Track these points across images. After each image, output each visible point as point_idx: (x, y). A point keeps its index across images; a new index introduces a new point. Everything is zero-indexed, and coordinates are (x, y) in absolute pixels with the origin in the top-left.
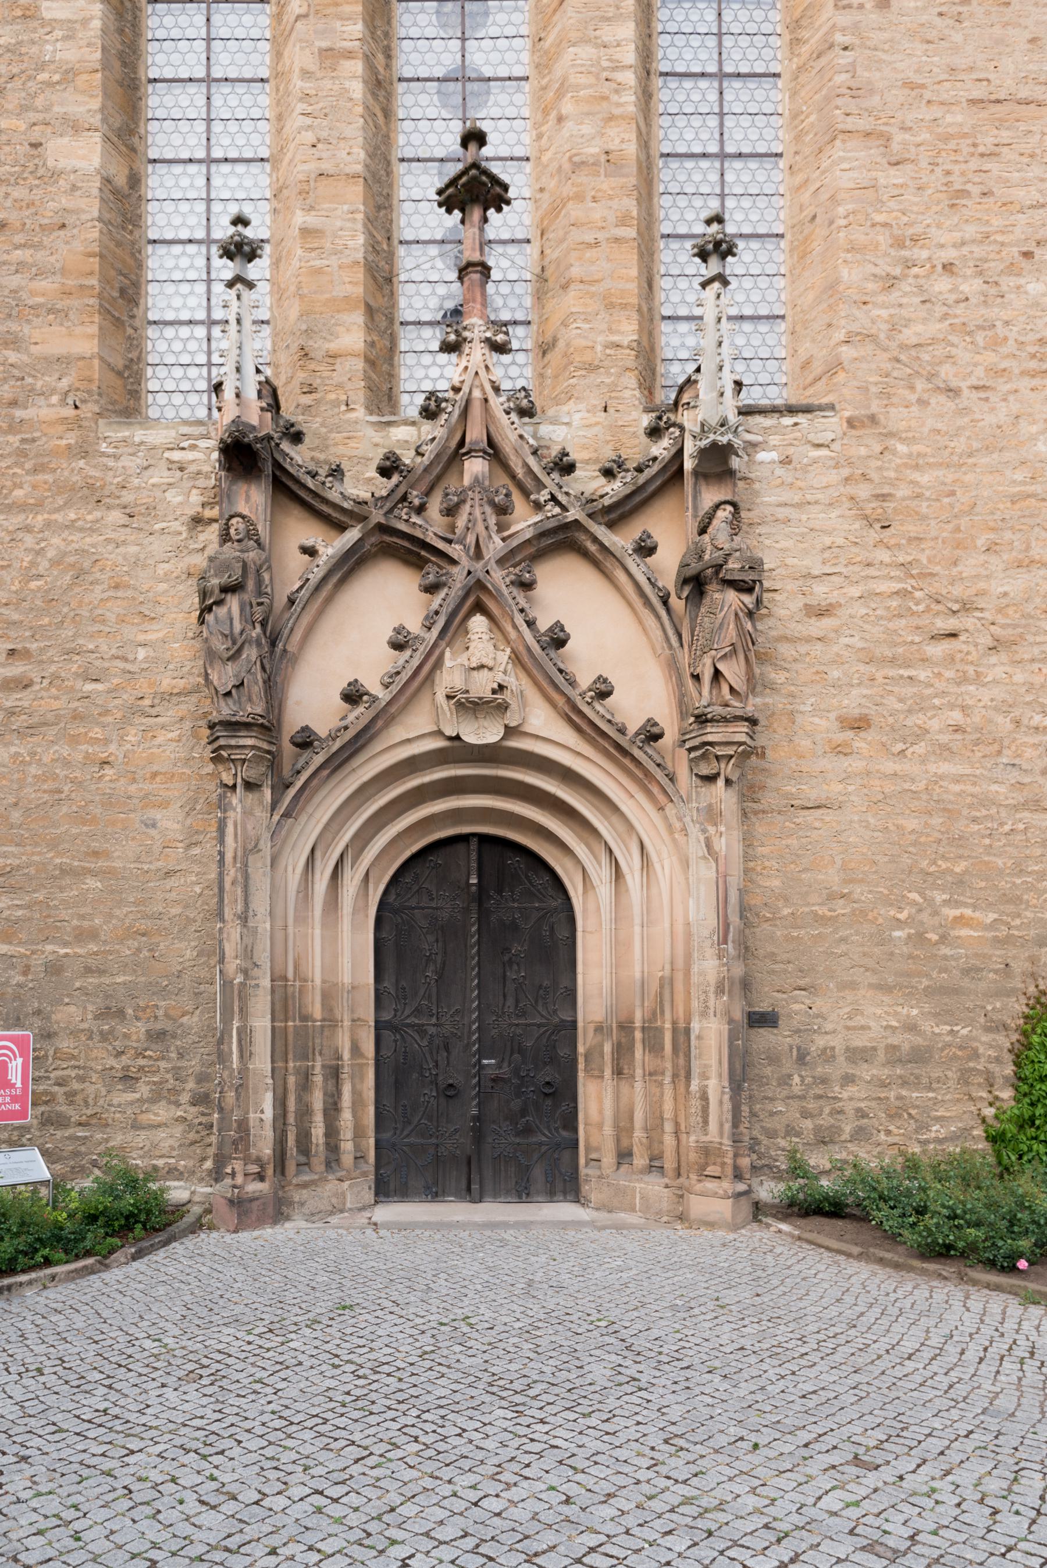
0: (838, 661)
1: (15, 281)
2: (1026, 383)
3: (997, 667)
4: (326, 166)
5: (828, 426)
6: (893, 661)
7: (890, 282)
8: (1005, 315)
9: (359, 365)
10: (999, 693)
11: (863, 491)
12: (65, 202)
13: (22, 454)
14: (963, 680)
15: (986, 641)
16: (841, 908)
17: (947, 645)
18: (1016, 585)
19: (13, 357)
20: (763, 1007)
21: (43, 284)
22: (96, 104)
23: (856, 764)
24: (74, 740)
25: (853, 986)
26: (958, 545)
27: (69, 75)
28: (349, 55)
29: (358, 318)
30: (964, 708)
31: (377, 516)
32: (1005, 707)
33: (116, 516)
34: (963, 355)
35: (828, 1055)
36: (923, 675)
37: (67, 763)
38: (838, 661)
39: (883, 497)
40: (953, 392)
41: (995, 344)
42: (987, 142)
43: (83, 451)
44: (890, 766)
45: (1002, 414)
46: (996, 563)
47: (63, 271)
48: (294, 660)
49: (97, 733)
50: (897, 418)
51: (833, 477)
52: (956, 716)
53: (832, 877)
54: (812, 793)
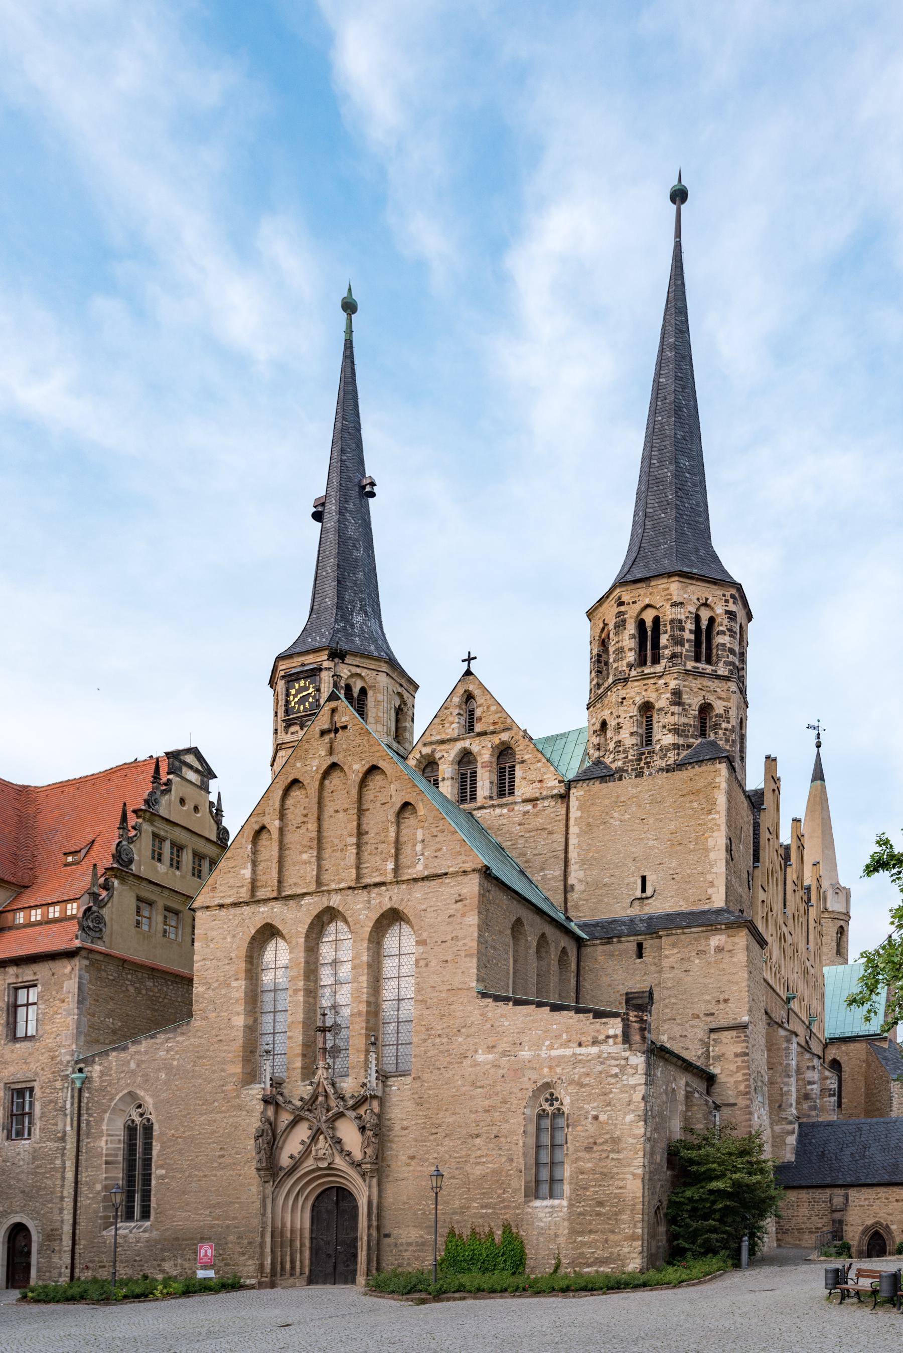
0: (408, 1141)
1: (224, 1054)
2: (457, 1065)
3: (447, 1142)
4: (294, 1020)
5: (409, 1079)
6: (422, 1141)
7: (425, 1041)
8: (453, 1047)
9: (299, 1071)
10: (446, 1148)
11: (416, 1096)
12: (235, 1034)
13: (224, 1098)
14: (438, 1145)
15: (444, 1135)
16: (407, 1206)
17: (434, 1136)
18: (451, 1120)
19: (223, 1074)
20: (387, 1232)
21: (230, 1055)
22: (243, 1008)
23: (411, 1168)
24: (234, 1170)
25: (408, 1226)
26: (438, 1109)
27: (237, 1001)
28: (300, 990)
29: (300, 1059)
30: (438, 1153)
31: (297, 1113)
32: (447, 1152)
33: (244, 1113)
34: (442, 1059)
35: (402, 1244)
36: (428, 1144)
37: (232, 1176)
38: (408, 1141)
39: (421, 1098)
40: (439, 1069)
41: (450, 1055)
42: (450, 1001)
43: (238, 1097)
44: (420, 1169)
45: (450, 1075)
46: (447, 1113)
47: (235, 1052)
48: (282, 1148)
49: (239, 1168)
50: (425, 1077)
51: (409, 1093)
52: (436, 1155)
53: (405, 1198)
54: (401, 1176)
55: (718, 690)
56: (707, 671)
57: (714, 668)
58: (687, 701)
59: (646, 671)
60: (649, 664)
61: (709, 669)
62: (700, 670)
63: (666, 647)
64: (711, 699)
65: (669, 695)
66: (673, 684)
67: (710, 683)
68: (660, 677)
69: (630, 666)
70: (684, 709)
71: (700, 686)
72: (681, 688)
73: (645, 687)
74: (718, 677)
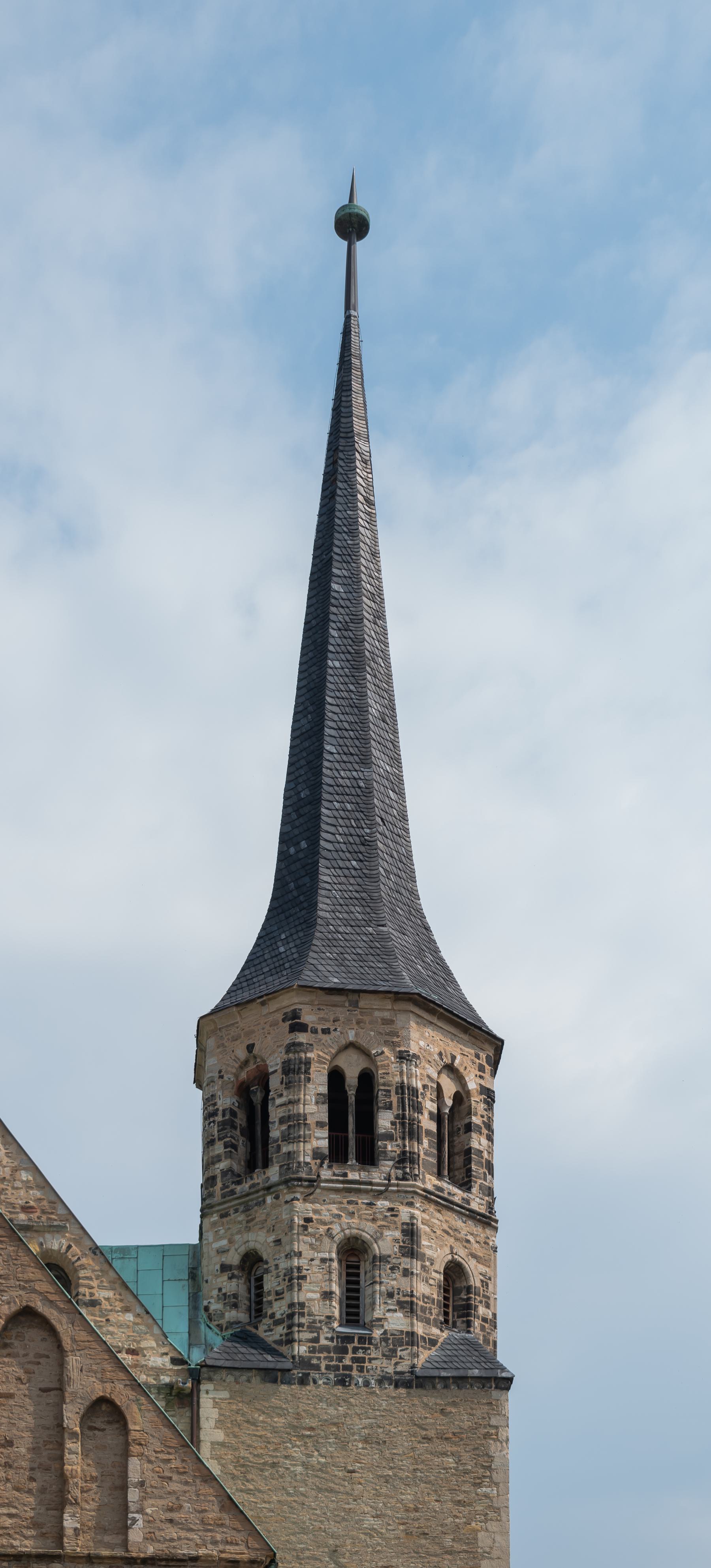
55: (470, 1238)
56: (456, 1199)
57: (465, 1195)
58: (429, 1252)
59: (352, 1176)
60: (352, 1161)
61: (458, 1195)
62: (446, 1195)
63: (390, 1137)
64: (462, 1254)
65: (398, 1234)
66: (405, 1212)
67: (459, 1223)
68: (379, 1194)
69: (317, 1154)
70: (423, 1267)
71: (445, 1227)
72: (421, 1226)
73: (351, 1208)
74: (473, 1216)
